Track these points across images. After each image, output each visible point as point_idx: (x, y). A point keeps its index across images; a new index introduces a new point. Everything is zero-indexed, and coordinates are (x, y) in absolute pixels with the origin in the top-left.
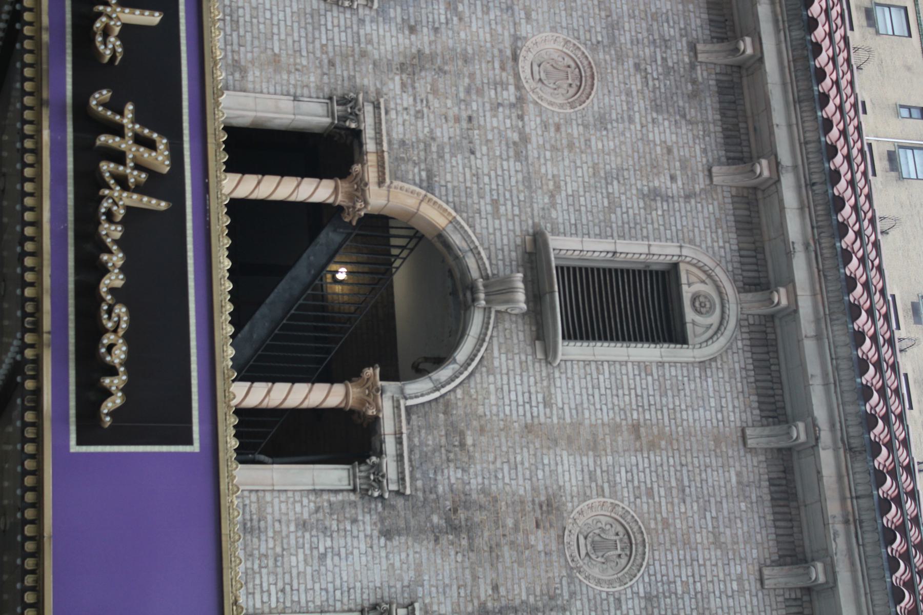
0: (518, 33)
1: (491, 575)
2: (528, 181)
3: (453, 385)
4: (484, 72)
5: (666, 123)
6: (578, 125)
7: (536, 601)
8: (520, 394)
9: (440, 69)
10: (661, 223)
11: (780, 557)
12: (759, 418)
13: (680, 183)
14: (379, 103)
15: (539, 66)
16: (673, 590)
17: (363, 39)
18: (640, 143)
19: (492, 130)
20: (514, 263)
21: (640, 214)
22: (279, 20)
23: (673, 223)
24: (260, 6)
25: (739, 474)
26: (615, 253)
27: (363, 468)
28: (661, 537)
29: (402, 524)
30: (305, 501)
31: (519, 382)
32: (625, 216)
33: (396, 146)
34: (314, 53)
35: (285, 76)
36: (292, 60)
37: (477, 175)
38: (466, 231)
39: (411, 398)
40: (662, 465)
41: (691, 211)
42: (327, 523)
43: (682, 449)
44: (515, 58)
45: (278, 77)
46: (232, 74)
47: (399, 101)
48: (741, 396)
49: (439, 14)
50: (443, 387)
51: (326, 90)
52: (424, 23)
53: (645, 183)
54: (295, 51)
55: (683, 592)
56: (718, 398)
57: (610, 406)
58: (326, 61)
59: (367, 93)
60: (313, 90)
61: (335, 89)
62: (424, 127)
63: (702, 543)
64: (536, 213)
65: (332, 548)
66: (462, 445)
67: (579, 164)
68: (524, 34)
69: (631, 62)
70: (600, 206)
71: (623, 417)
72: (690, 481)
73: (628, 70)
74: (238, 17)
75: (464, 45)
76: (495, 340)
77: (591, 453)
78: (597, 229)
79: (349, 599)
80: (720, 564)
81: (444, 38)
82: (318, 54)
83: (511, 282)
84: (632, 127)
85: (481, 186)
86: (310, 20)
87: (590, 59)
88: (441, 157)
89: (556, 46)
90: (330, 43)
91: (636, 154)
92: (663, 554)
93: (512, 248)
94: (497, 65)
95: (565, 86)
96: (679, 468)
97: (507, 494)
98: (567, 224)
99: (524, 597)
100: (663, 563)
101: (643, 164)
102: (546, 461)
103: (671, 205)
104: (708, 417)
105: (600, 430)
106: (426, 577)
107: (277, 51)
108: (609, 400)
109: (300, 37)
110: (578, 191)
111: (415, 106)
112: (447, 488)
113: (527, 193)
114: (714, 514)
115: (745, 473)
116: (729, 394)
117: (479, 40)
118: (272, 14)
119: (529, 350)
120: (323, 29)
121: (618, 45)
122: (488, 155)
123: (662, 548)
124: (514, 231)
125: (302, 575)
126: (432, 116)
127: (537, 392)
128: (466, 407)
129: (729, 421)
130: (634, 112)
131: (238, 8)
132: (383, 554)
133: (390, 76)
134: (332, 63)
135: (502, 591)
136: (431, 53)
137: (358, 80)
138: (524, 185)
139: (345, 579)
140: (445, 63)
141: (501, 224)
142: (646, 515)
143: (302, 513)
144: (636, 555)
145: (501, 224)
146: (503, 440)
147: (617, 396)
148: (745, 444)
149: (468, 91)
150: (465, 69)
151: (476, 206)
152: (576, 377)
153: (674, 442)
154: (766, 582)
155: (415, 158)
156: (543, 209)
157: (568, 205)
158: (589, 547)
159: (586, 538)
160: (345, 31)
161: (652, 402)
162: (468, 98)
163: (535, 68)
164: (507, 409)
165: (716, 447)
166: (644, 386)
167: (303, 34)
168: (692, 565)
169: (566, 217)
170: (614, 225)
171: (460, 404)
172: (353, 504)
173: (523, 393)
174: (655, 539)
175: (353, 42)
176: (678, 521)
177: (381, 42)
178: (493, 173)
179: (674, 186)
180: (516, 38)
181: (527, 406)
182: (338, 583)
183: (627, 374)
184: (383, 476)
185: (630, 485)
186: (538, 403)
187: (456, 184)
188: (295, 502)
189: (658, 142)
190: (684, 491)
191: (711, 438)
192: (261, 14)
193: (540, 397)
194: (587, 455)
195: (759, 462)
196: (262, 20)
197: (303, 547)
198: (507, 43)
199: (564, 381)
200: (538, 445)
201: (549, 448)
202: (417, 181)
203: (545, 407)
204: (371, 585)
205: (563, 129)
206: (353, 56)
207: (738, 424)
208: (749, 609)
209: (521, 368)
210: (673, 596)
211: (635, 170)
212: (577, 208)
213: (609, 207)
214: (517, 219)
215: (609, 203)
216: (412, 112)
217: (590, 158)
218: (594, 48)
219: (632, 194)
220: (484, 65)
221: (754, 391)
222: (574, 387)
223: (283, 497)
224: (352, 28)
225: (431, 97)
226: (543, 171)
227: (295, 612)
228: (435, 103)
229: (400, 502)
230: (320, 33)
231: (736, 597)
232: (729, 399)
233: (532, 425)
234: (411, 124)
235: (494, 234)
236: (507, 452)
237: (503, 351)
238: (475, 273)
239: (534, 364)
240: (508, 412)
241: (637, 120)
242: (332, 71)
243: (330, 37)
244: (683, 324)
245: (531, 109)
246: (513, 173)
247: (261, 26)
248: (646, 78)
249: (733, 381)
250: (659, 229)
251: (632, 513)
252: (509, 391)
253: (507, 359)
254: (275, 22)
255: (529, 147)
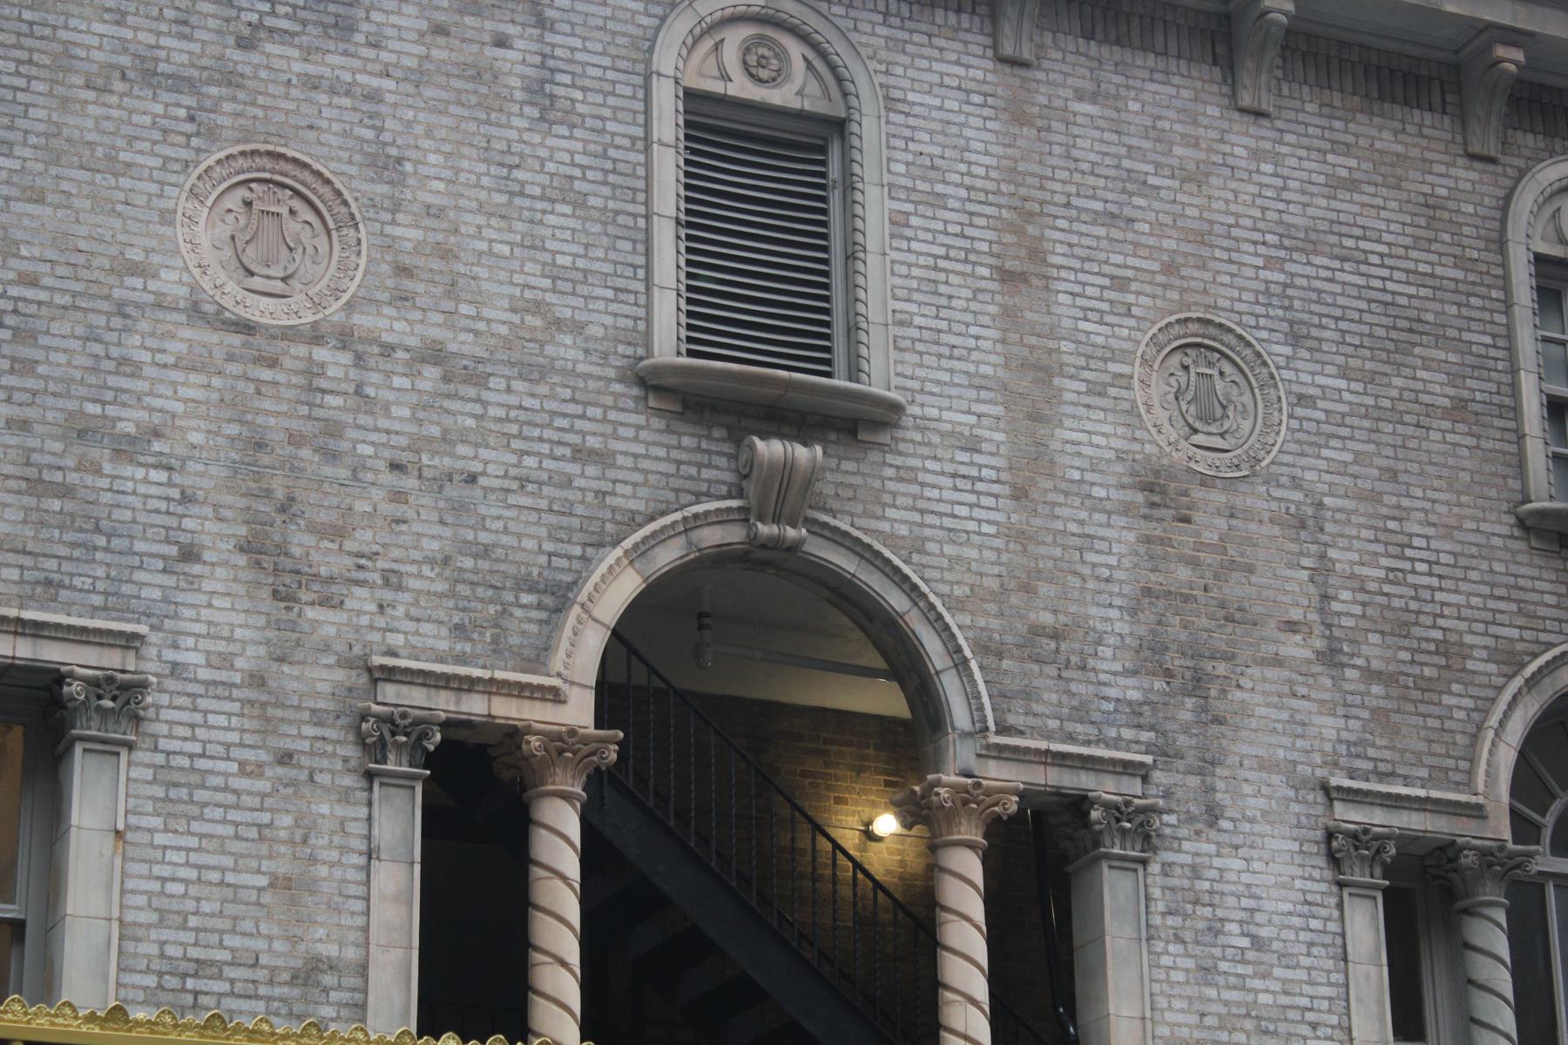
0: (182, 304)
1: (1271, 629)
2: (533, 372)
3: (955, 630)
4: (284, 408)
5: (376, 16)
6: (394, 222)
7: (1308, 555)
8: (958, 496)
9: (282, 510)
10: (599, 99)
11: (1215, 63)
12: (977, 19)
13: (511, 30)
14: (382, 668)
15: (252, 274)
16: (1279, 289)
17: (222, 676)
18: (429, 92)
19: (420, 422)
20: (704, 445)
21: (586, 142)
22: (187, 864)
23: (598, 72)
24: (155, 903)
25: (1080, 96)
26: (678, 222)
27: (1107, 841)
28: (1193, 284)
29: (1194, 781)
30: (1166, 960)
31: (935, 494)
32: (590, 175)
33: (468, 648)
34: (263, 796)
35: (323, 871)
36: (283, 849)
37: (523, 481)
38: (654, 534)
39: (984, 719)
40: (1070, 245)
41: (573, 25)
42: (1201, 925)
43: (1039, 195)
44: (245, 328)
45: (325, 887)
46: (326, 990)
47: (365, 620)
48: (936, 41)
49: (146, 481)
50: (959, 650)
51: (349, 781)
52: (172, 522)
53: (516, 108)
54: (261, 839)
55: (1282, 270)
56: (943, 91)
57: (969, 318)
58: (280, 770)
59: (350, 690)
60: (350, 812)
61: (346, 760)
62: (420, 576)
63: (1201, 208)
64: (596, 370)
65: (1241, 922)
66: (1056, 636)
67: (483, 246)
68: (183, 291)
69: (237, 55)
70: (572, 223)
71: (988, 297)
72: (1094, 197)
73: (257, 66)
74: (185, 958)
75: (220, 440)
76: (859, 522)
77: (1057, 381)
78: (621, 244)
79: (1321, 905)
80: (1234, 185)
81: (206, 483)
82: (263, 785)
83: (772, 466)
84: (391, 99)
85: (545, 476)
86: (183, 793)
87: (235, 150)
88: (485, 552)
89: (202, 221)
90: (236, 753)
91: (453, 109)
92: (1223, 291)
93: (673, 440)
94: (266, 374)
95: (292, 227)
96: (1074, 213)
97: (1136, 566)
98: (614, 307)
99: (1305, 575)
100: (1236, 294)
101: (473, 100)
102: (1077, 475)
103: (561, 65)
104: (980, 123)
105: (1016, 350)
106: (1281, 753)
107: (263, 881)
108: (958, 316)
109: (224, 821)
110: (544, 264)
111: (373, 586)
112: (1131, 681)
113: (556, 379)
114: (1150, 168)
115: (1079, 83)
116: (935, 66)
117: (207, 403)
118: (174, 880)
119: (874, 456)
120: (201, 764)
121: (196, 74)
122: (477, 445)
123: (1212, 289)
124: (639, 428)
125: (1289, 987)
126: (396, 553)
127: (952, 460)
128: (987, 613)
129: (984, 82)
130: (355, 83)
131: (162, 955)
132: (1247, 827)
133: (307, 629)
134: (285, 758)
135: (1296, 614)
136: (247, 522)
137: (322, 705)
138: (538, 382)
139: (1289, 907)
140: (268, 494)
141: (626, 454)
142: (1159, 303)
143: (1187, 970)
144: (1221, 342)
145: (626, 454)
146: (1042, 550)
147: (950, 297)
148: (1025, 65)
149: (332, 456)
150: (278, 451)
151: (590, 497)
152: (920, 373)
153: (1028, 206)
154: (1264, 106)
155: (492, 609)
156: (587, 351)
157: (574, 294)
158: (1213, 429)
159: (1196, 431)
160: (206, 712)
161: (957, 229)
162: (348, 460)
163: (257, 283)
164: (985, 528)
165: (1032, 125)
166: (929, 237)
167: (218, 813)
168: (1236, 240)
169: (600, 305)
170: (611, 205)
171: (982, 622)
172: (1167, 869)
173: (955, 488)
174: (1198, 298)
175: (230, 699)
176: (1166, 244)
177: (226, 633)
178: (517, 444)
179: (520, 44)
180: (195, 311)
181: (980, 486)
182: (1296, 921)
183: (910, 265)
184: (1127, 804)
185: (1108, 319)
186: (972, 464)
187: (543, 532)
188: (1168, 981)
189: (422, 50)
190: (1113, 215)
191: (1014, 130)
192: (174, 907)
193: (963, 457)
194: (1061, 390)
195: (1057, 47)
196: (190, 905)
197: (1242, 976)
198: (214, 338)
199: (928, 399)
200: (1049, 484)
201: (1052, 461)
202: (543, 615)
203: (979, 451)
204: (1298, 859)
205: (407, 261)
206: (264, 705)
207: (989, 65)
208: (1303, 153)
209: (909, 481)
210: (1289, 292)
211: (488, 122)
212: (580, 276)
213: (575, 205)
214: (612, 415)
215: (564, 201)
216: (388, 595)
217: (468, 217)
218: (212, 134)
219: (542, 145)
220: (267, 405)
221: (927, 11)
222: (938, 382)
223: (1162, 1002)
224: (195, 696)
225: (349, 545)
226: (504, 330)
227: (1348, 1008)
228: (363, 539)
229: (1157, 776)
230: (211, 772)
231: (1285, 172)
232: (945, 68)
233: (1014, 486)
234: (417, 603)
235: (646, 472)
236: (1064, 548)
237: (879, 512)
238: (733, 535)
239: (901, 454)
240: (992, 529)
241: (375, 82)
242: (305, 761)
243: (221, 750)
244: (800, 115)
245: (363, 321)
246: (512, 400)
247: (206, 907)
248: (271, 30)
249: (909, 48)
250: (615, 109)
251: (1154, 330)
252: (954, 516)
253: (894, 506)
254: (192, 874)
255: (452, 347)
